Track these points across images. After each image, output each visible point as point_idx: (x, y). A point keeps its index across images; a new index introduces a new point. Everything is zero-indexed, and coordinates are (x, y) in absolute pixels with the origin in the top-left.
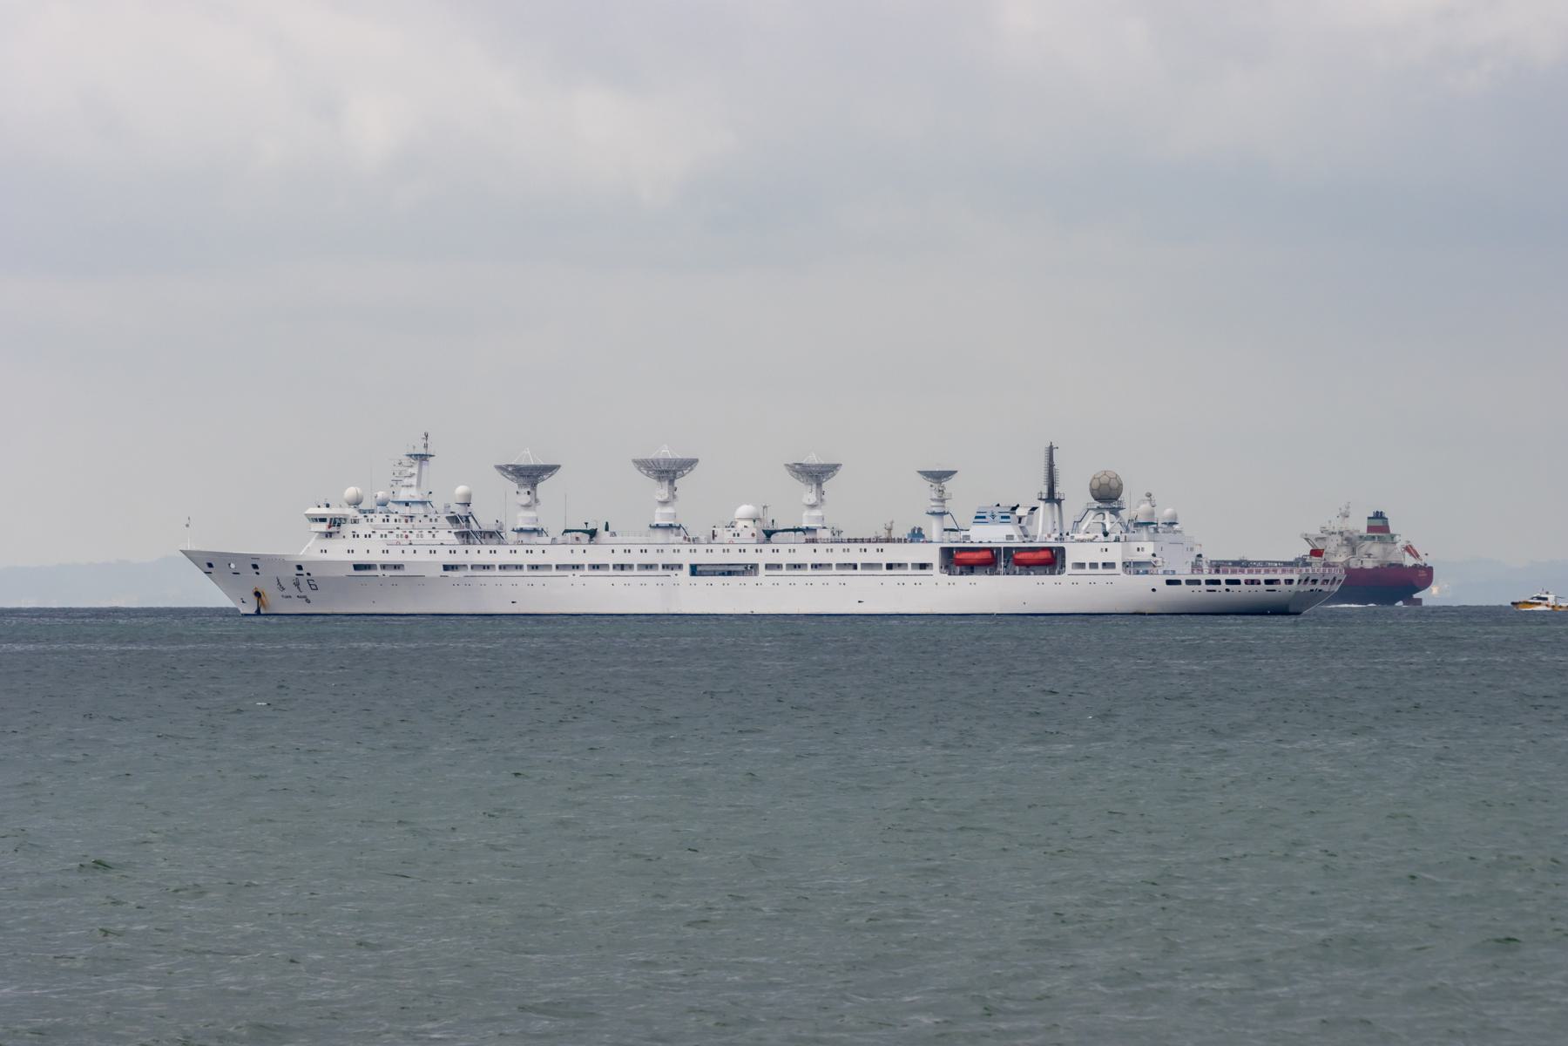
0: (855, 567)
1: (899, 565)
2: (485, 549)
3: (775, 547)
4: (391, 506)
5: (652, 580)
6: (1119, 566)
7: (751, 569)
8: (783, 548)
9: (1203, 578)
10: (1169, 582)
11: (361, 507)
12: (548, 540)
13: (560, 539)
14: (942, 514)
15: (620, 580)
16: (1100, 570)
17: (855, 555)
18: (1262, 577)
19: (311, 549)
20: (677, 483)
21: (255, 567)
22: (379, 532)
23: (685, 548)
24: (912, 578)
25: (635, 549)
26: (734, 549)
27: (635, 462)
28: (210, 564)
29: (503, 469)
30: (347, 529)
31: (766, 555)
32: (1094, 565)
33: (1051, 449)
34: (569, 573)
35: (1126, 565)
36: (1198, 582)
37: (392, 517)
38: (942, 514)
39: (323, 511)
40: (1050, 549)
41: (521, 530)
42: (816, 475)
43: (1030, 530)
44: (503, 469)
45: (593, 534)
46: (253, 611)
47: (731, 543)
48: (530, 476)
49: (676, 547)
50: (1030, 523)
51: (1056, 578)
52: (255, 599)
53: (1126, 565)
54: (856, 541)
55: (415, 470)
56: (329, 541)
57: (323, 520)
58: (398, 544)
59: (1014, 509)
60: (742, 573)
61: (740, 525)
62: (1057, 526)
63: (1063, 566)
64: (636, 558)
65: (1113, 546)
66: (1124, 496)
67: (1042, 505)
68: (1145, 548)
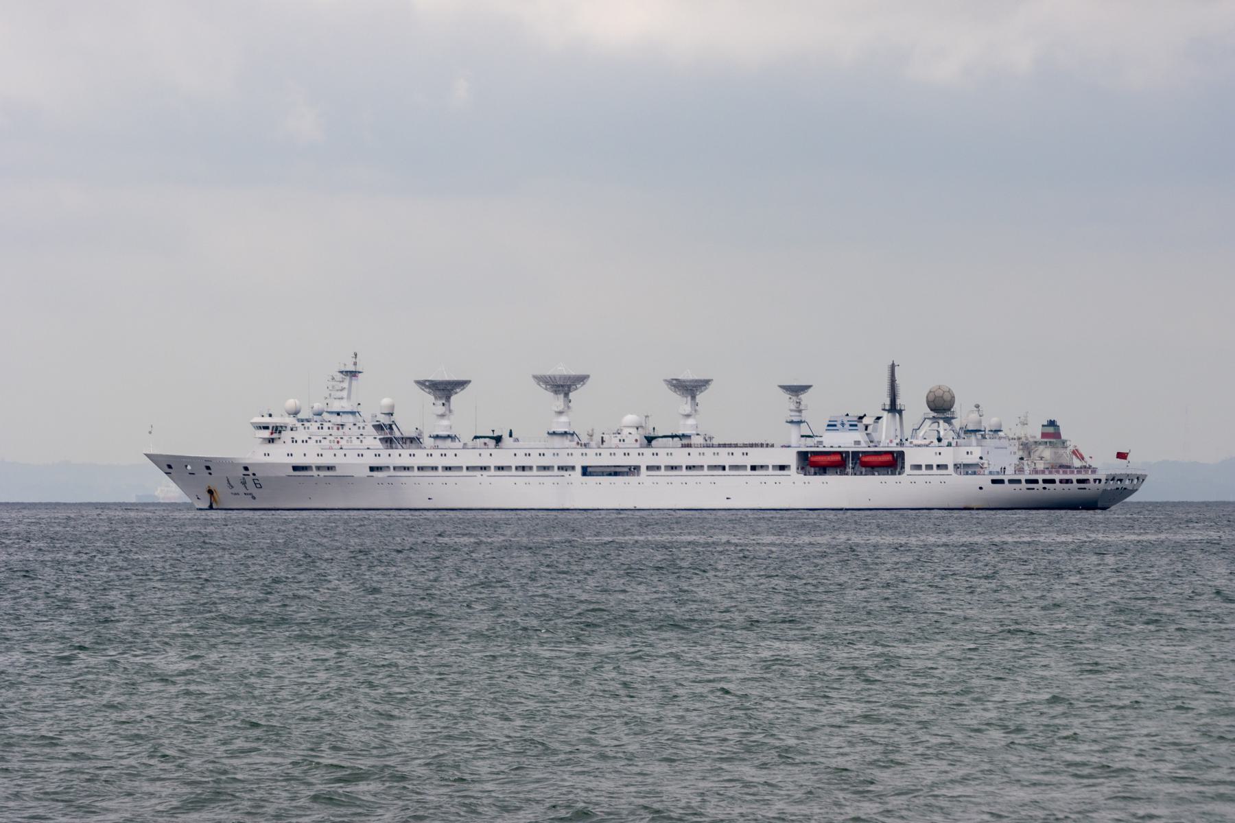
0: (724, 468)
1: (762, 467)
2: (405, 452)
3: (655, 451)
4: (325, 414)
5: (548, 480)
6: (951, 467)
7: (633, 470)
8: (662, 452)
9: (1023, 478)
10: (994, 482)
11: (300, 416)
12: (460, 445)
13: (470, 444)
14: (800, 422)
15: (521, 479)
16: (935, 471)
17: (724, 458)
18: (1074, 477)
19: (254, 452)
20: (571, 395)
21: (208, 468)
22: (314, 438)
23: (578, 452)
24: (772, 477)
25: (534, 453)
26: (620, 452)
27: (535, 377)
28: (169, 465)
29: (421, 383)
30: (287, 435)
31: (646, 458)
32: (929, 467)
33: (893, 367)
34: (478, 473)
35: (956, 466)
36: (1019, 481)
37: (326, 425)
38: (800, 422)
39: (267, 420)
40: (891, 453)
41: (437, 437)
42: (690, 389)
43: (875, 436)
44: (421, 383)
45: (498, 439)
46: (206, 506)
47: (617, 447)
48: (444, 390)
49: (570, 451)
50: (875, 430)
51: (896, 478)
52: (208, 496)
53: (956, 466)
54: (725, 446)
55: (345, 385)
56: (271, 445)
57: (266, 428)
58: (331, 448)
59: (861, 418)
61: (625, 431)
62: (898, 433)
63: (903, 467)
64: (535, 461)
65: (945, 450)
66: (956, 408)
67: (885, 415)
68: (972, 452)
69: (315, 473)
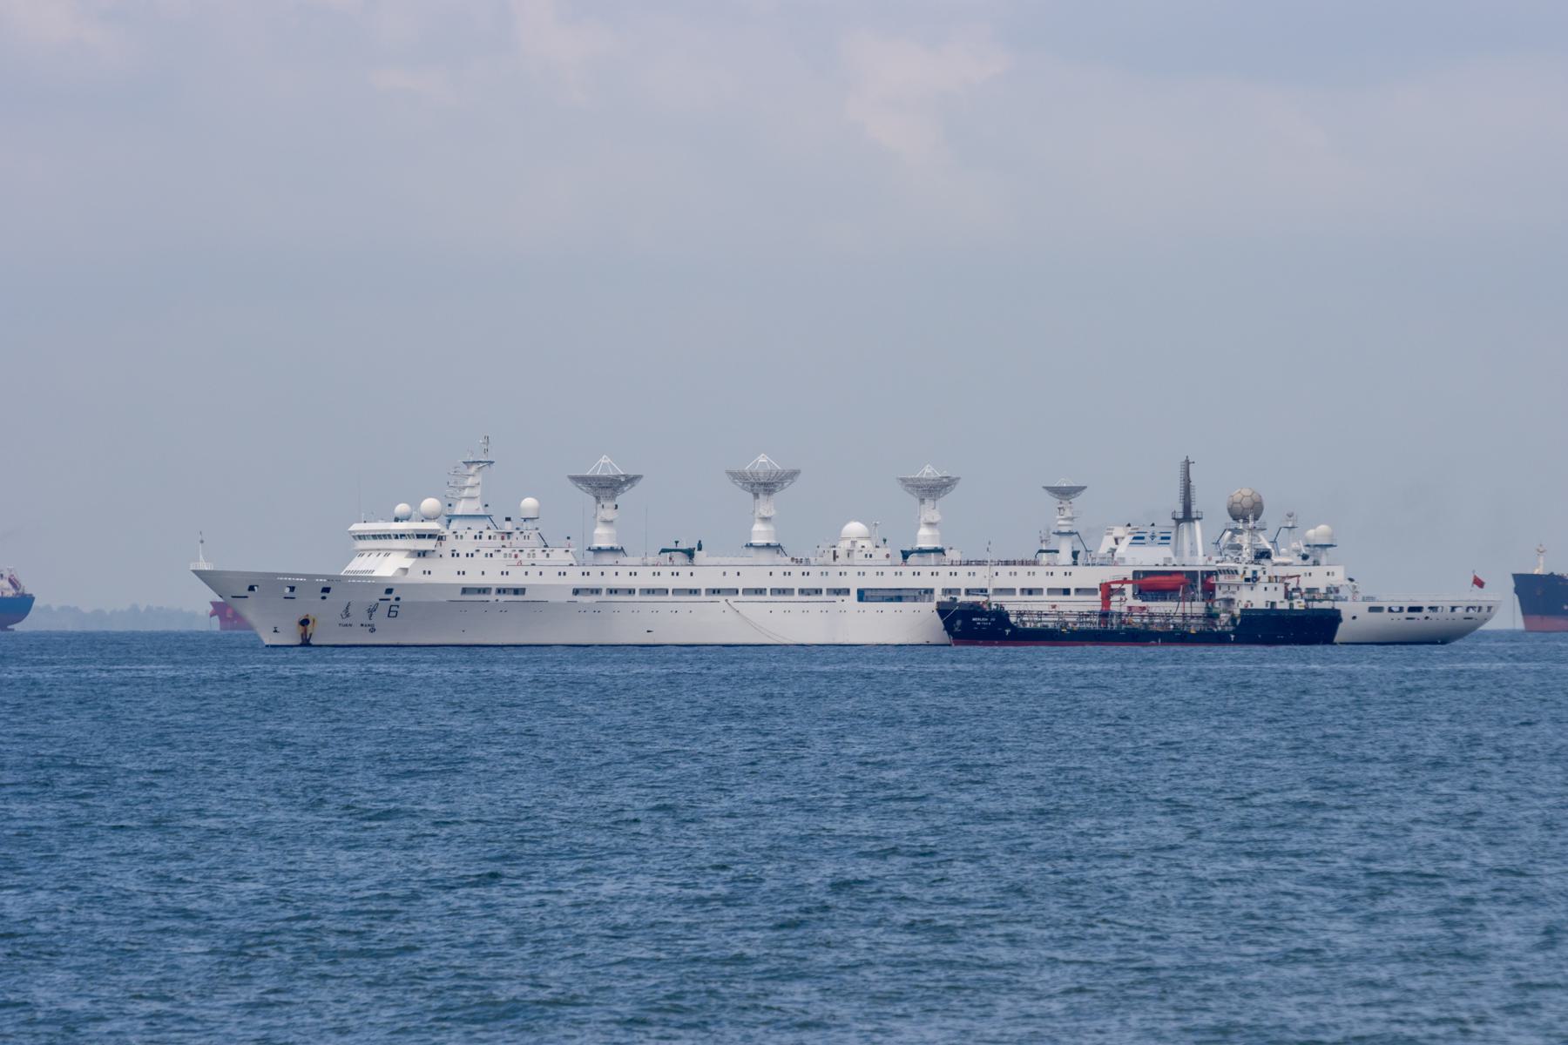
5: (814, 606)
10: (1372, 609)
15: (780, 606)
60: (915, 599)
69: (492, 597)
